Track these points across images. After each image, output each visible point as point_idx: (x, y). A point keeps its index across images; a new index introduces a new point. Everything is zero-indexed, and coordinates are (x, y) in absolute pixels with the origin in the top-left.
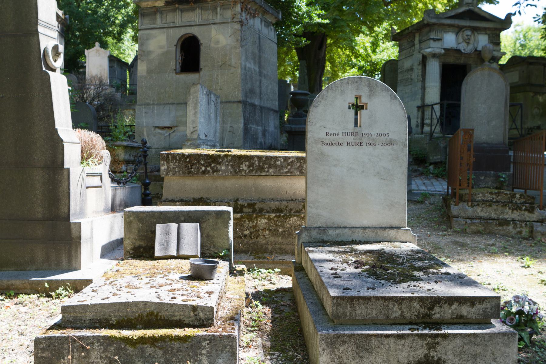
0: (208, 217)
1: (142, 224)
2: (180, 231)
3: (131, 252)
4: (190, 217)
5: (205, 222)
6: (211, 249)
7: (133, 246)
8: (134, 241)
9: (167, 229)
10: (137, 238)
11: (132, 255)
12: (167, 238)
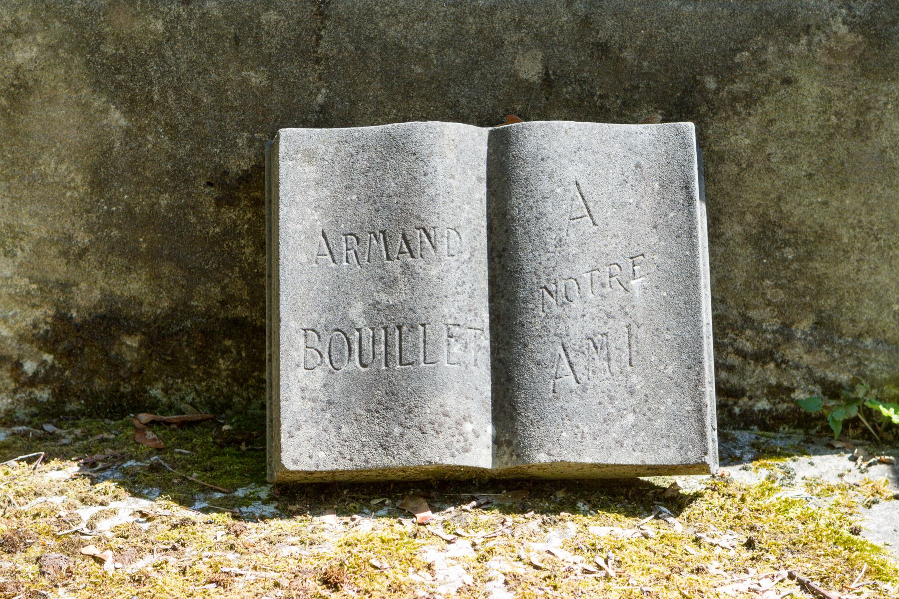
0: (783, 54)
1: (131, 106)
2: (518, 203)
3: (30, 367)
4: (603, 48)
5: (750, 100)
6: (796, 353)
7: (43, 313)
8: (59, 269)
9: (391, 185)
10: (82, 238)
11: (43, 394)
12: (390, 284)
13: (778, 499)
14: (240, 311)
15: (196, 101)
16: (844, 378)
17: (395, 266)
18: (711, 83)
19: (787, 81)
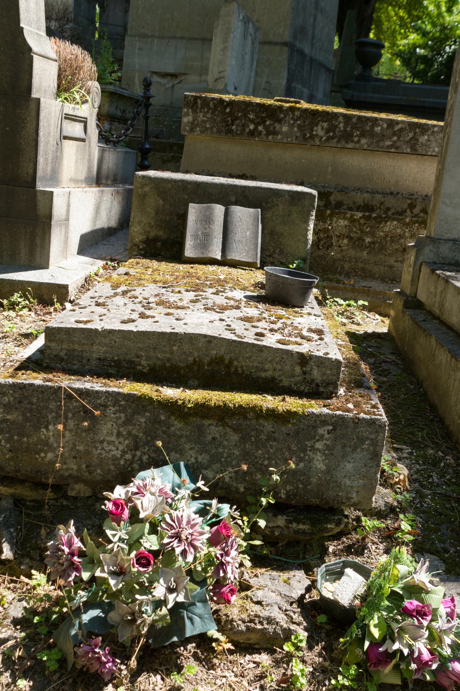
0: (277, 200)
1: (164, 200)
3: (141, 247)
4: (246, 197)
5: (271, 208)
6: (276, 256)
7: (144, 237)
8: (148, 229)
9: (208, 214)
10: (153, 224)
11: (143, 252)
12: (206, 229)
13: (275, 312)
14: (179, 240)
15: (175, 200)
16: (284, 261)
17: (207, 226)
18: (264, 205)
19: (277, 205)
